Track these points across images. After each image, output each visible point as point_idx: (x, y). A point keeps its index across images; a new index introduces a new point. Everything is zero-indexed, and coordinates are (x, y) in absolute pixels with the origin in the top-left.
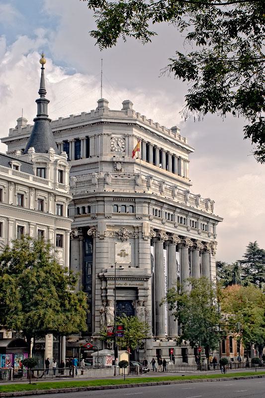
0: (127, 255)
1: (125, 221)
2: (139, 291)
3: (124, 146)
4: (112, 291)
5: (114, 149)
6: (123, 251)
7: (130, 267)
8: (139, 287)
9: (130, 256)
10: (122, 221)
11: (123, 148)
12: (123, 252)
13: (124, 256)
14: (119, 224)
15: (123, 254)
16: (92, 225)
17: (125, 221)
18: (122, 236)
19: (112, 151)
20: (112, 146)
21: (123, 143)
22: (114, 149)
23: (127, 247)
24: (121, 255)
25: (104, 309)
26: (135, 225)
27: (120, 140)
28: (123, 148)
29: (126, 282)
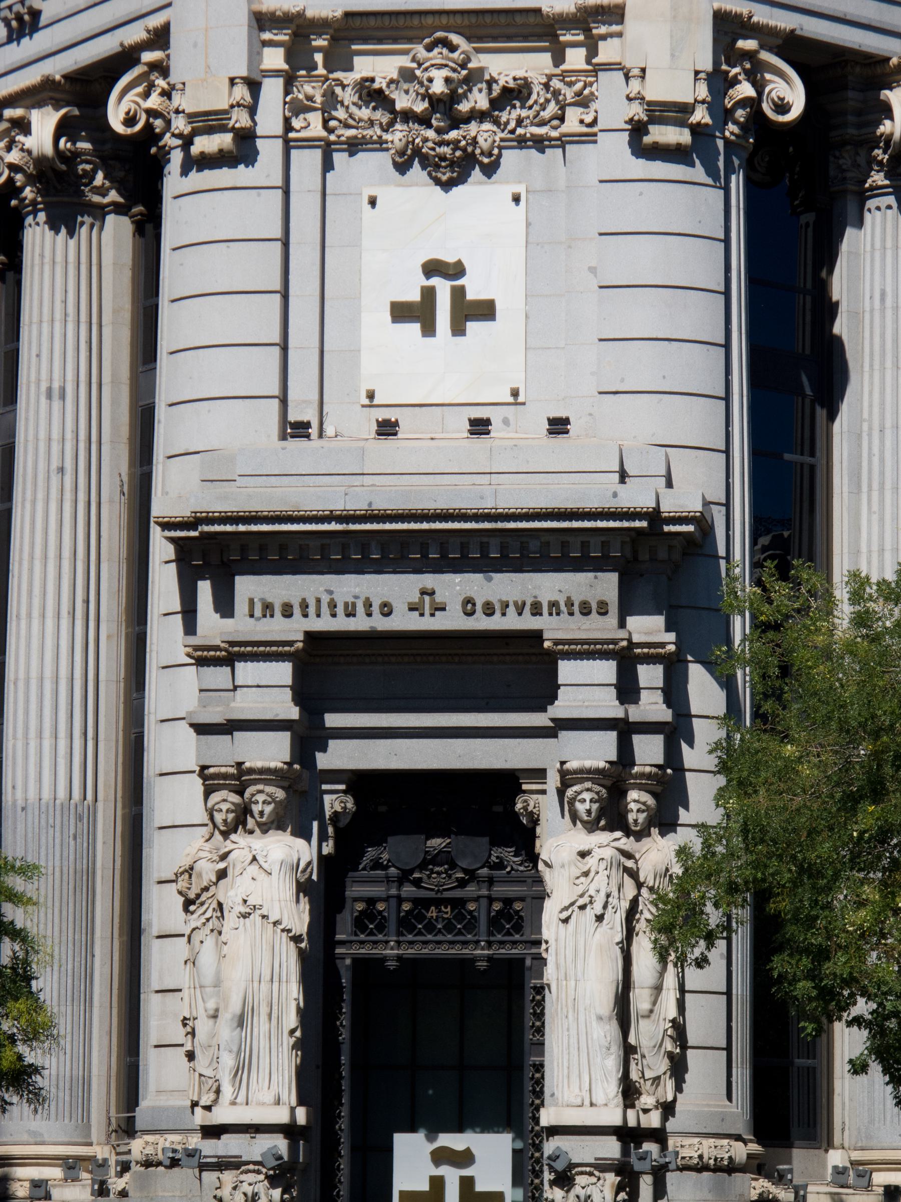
0: (485, 311)
2: (567, 670)
4: (282, 672)
6: (432, 268)
7: (480, 427)
8: (554, 629)
12: (443, 288)
13: (458, 330)
16: (135, 34)
18: (424, 121)
24: (416, 313)
25: (207, 870)
29: (429, 580)
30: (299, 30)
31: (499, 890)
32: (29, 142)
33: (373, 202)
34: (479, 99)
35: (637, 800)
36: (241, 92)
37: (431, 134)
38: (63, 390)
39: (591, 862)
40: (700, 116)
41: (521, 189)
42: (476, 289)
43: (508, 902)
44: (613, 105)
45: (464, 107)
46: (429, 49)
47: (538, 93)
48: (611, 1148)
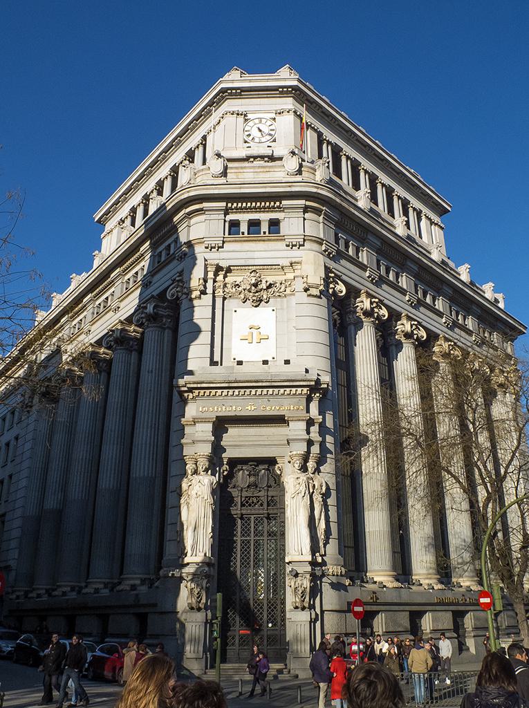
1: (257, 255)
3: (271, 132)
5: (251, 138)
9: (272, 341)
10: (249, 255)
11: (270, 135)
14: (243, 263)
15: (254, 334)
17: (257, 255)
19: (246, 142)
20: (247, 133)
21: (271, 127)
22: (251, 138)
23: (265, 316)
26: (286, 263)
27: (264, 121)
28: (270, 135)
30: (218, 269)
31: (270, 494)
32: (147, 311)
33: (236, 311)
34: (264, 286)
35: (311, 464)
36: (202, 281)
37: (251, 294)
38: (152, 371)
39: (300, 480)
40: (322, 287)
41: (274, 308)
42: (263, 331)
43: (272, 497)
44: (299, 285)
45: (260, 287)
46: (251, 273)
47: (278, 285)
48: (309, 569)
